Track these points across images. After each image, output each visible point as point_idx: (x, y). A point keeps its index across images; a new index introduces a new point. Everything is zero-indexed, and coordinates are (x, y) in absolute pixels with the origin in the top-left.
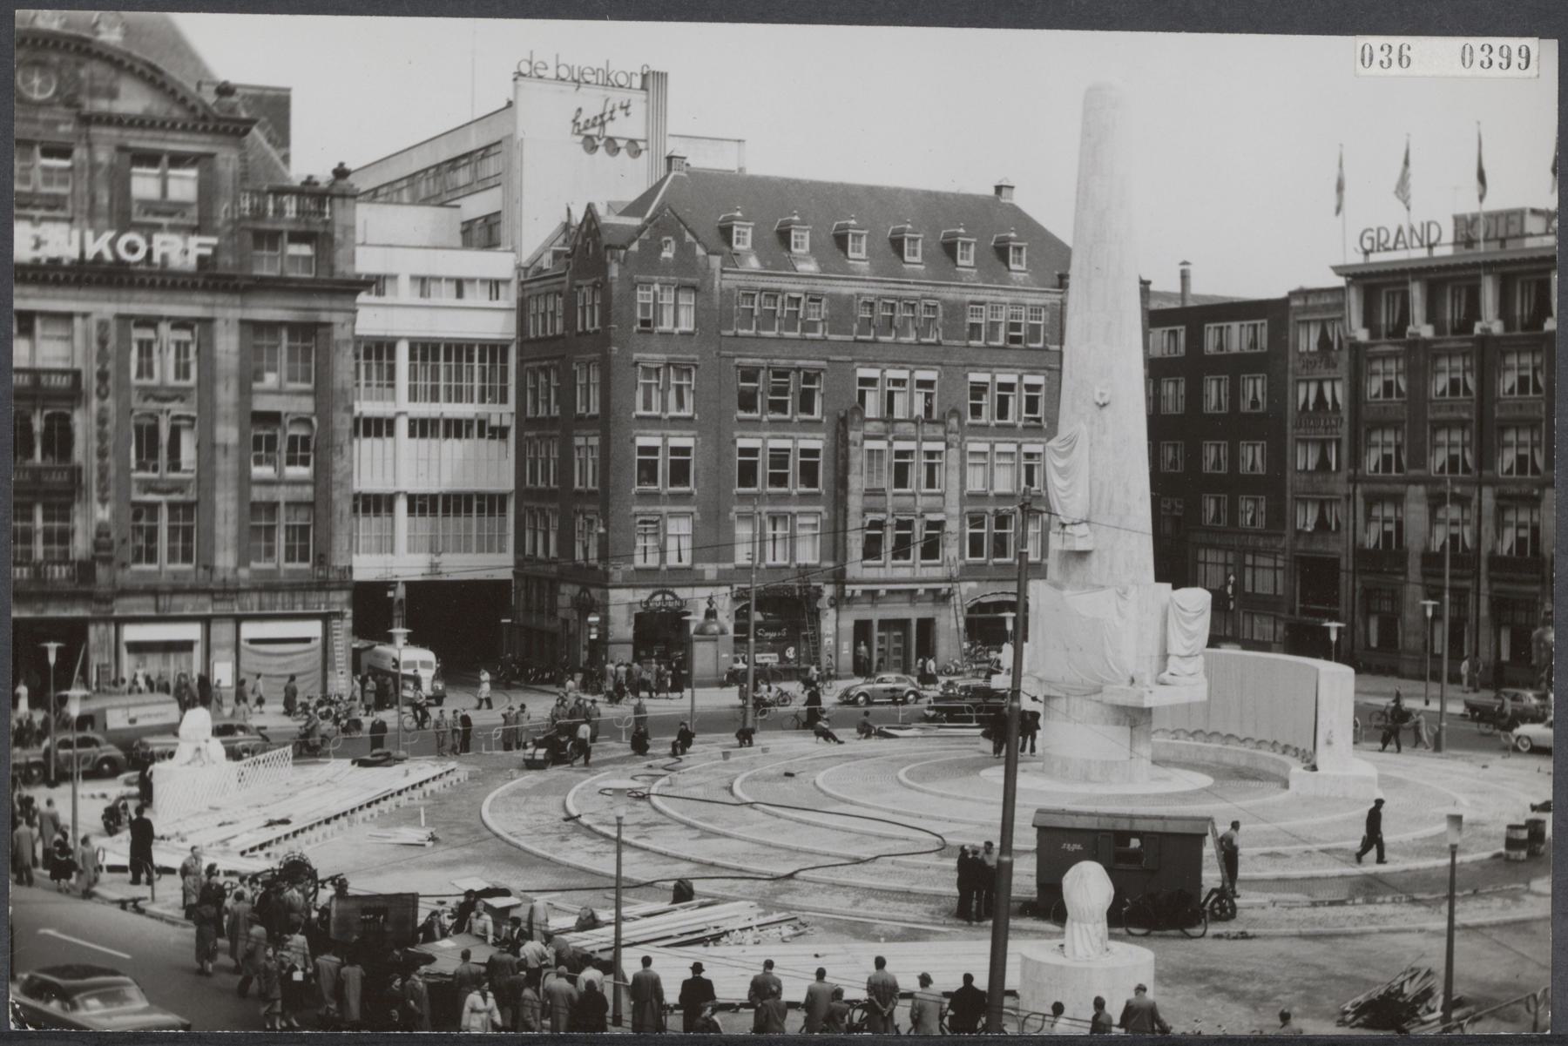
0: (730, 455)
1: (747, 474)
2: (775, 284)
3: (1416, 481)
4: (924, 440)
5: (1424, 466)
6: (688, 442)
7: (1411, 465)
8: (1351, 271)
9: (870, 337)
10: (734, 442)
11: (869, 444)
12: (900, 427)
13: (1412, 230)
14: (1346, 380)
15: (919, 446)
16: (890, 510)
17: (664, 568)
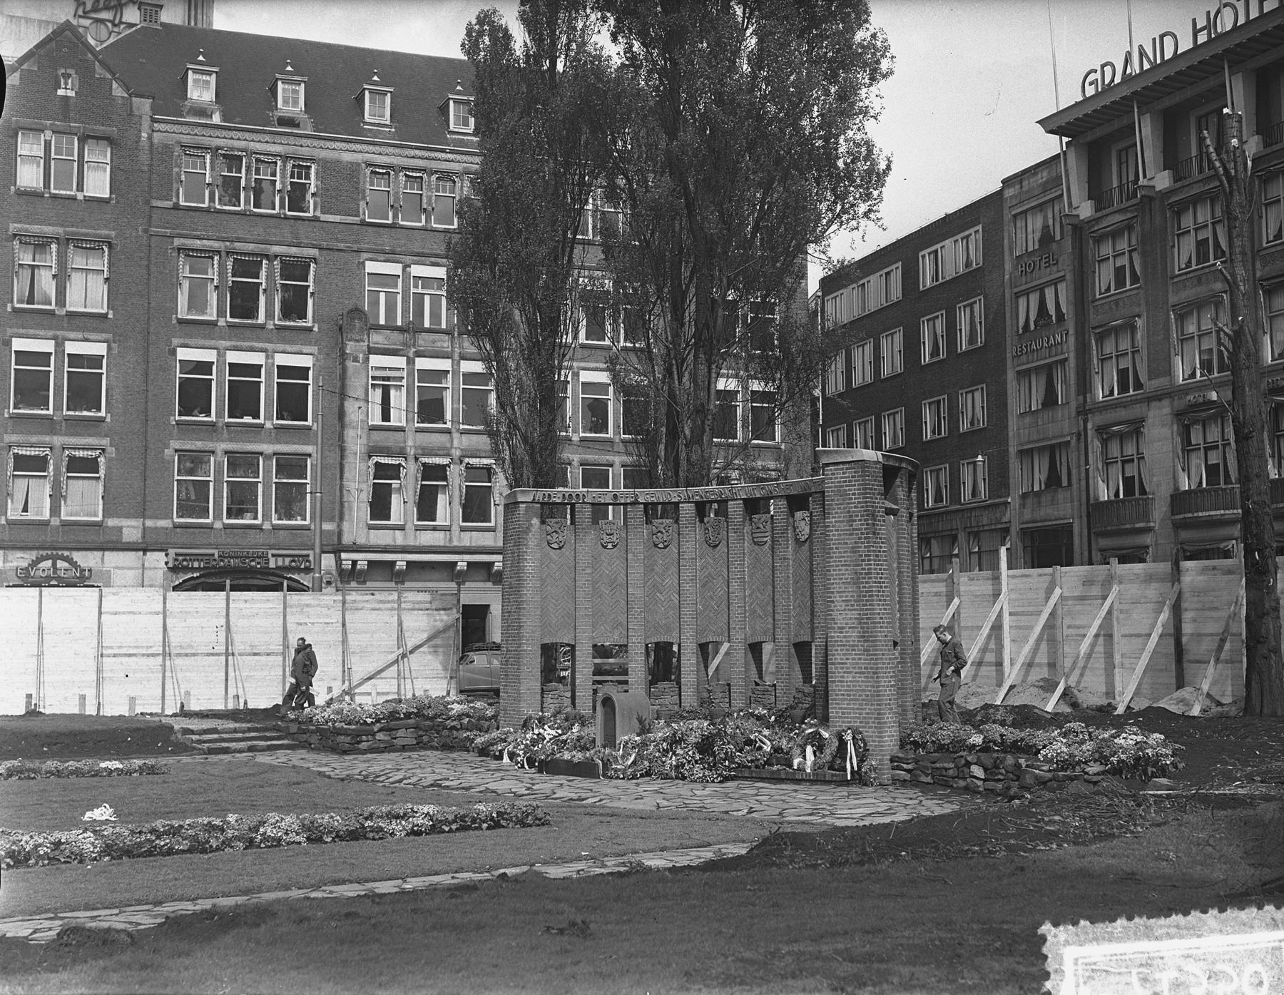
0: (169, 369)
1: (194, 395)
2: (237, 142)
3: (1157, 397)
4: (463, 357)
5: (1169, 372)
6: (99, 349)
7: (1152, 375)
8: (1062, 122)
9: (390, 222)
10: (174, 353)
11: (375, 360)
12: (423, 340)
13: (1142, 53)
14: (1068, 277)
15: (456, 365)
16: (411, 452)
17: (55, 522)
